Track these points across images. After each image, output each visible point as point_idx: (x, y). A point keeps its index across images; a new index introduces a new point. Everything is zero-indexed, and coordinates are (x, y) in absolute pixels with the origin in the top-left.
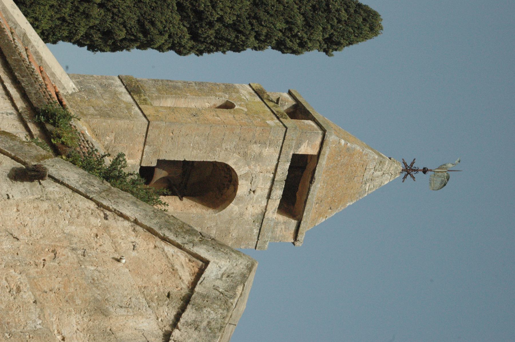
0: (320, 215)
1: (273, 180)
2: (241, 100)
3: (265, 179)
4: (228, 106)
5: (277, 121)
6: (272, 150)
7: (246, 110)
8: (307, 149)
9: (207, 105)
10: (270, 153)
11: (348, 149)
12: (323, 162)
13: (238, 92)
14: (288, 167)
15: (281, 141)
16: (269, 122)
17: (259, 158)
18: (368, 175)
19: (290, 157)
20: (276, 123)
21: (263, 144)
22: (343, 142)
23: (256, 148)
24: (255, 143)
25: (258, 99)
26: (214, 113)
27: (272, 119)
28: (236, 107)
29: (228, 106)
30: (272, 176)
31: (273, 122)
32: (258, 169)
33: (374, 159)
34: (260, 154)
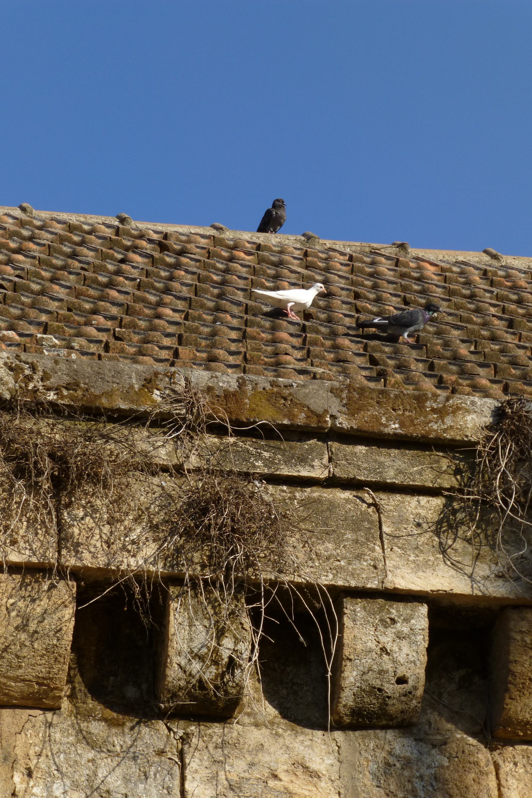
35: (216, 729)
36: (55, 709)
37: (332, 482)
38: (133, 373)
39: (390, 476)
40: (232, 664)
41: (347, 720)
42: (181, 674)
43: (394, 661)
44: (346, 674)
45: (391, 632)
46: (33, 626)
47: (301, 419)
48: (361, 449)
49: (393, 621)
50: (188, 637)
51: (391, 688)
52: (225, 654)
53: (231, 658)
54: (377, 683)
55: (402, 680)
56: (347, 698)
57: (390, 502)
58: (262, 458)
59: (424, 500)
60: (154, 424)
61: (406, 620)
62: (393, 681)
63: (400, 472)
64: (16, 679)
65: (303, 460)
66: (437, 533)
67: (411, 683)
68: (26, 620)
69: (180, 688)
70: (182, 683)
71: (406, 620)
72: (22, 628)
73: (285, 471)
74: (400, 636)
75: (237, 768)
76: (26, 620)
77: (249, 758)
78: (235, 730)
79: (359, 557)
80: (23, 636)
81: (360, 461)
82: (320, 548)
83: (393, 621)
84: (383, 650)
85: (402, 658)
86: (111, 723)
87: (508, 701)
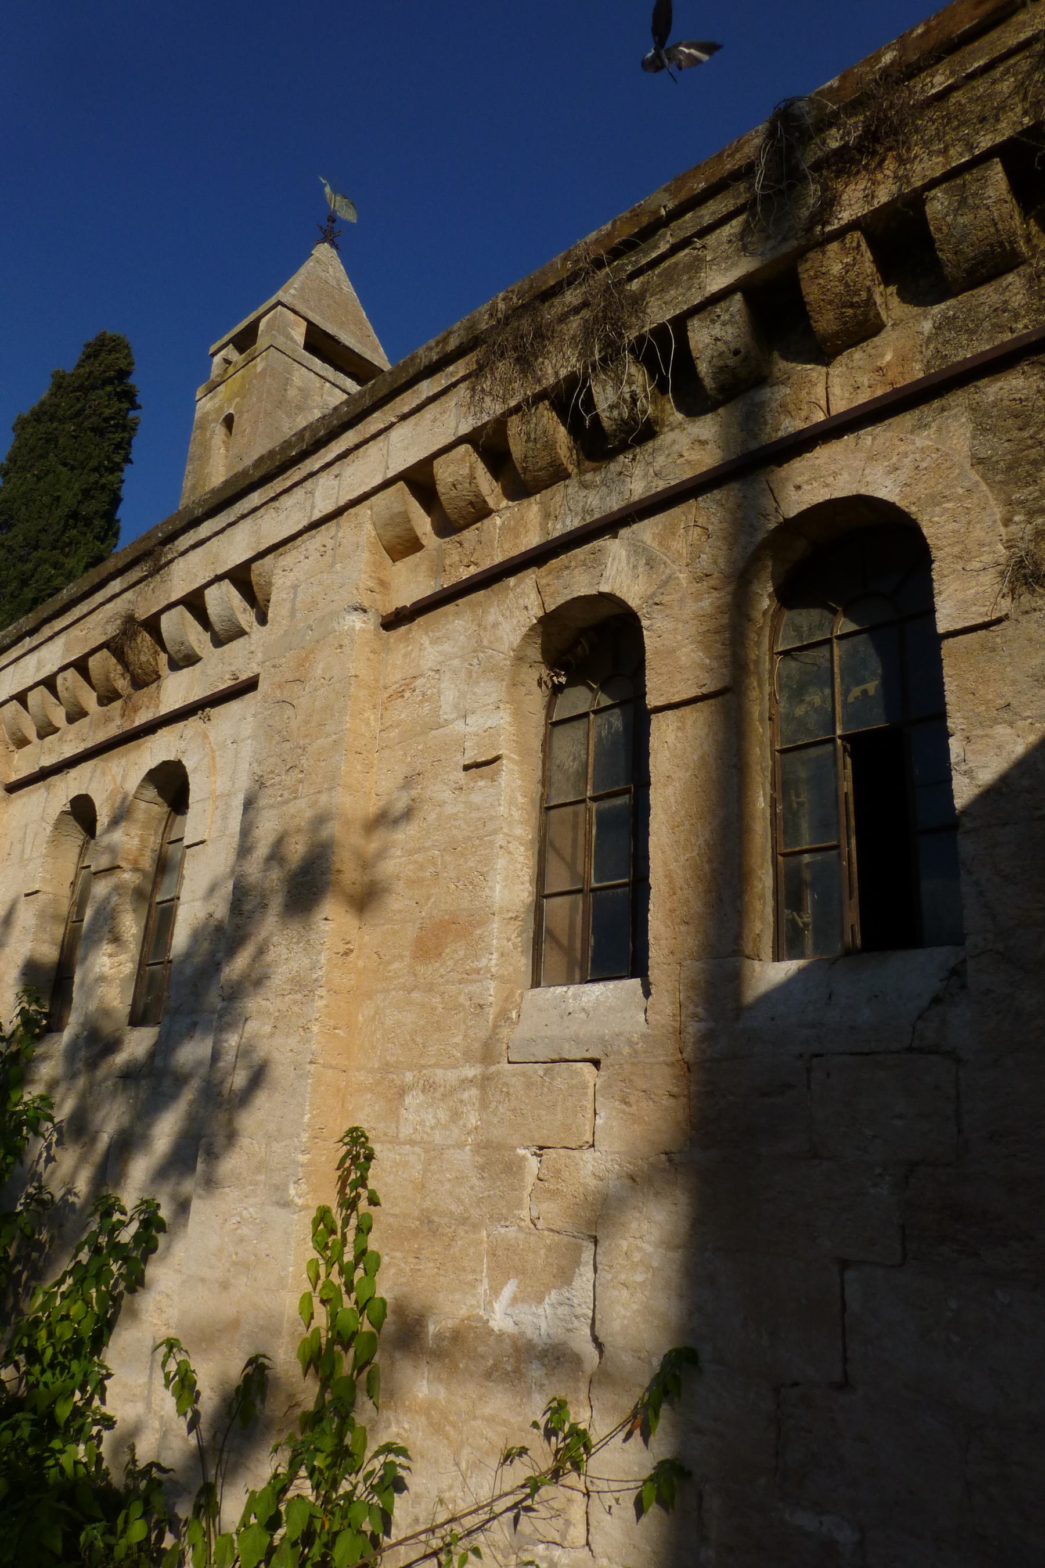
0: (376, 350)
1: (333, 384)
2: (221, 408)
3: (331, 394)
4: (229, 422)
5: (258, 359)
6: (296, 374)
7: (237, 399)
8: (299, 333)
9: (222, 451)
10: (300, 377)
11: (302, 289)
12: (317, 320)
13: (208, 413)
14: (319, 362)
15: (287, 358)
16: (259, 369)
17: (305, 392)
18: (334, 283)
19: (307, 354)
20: (262, 360)
21: (287, 382)
22: (292, 291)
23: (292, 393)
24: (285, 390)
25: (221, 388)
26: (239, 437)
27: (255, 366)
28: (232, 411)
29: (229, 422)
30: (328, 384)
31: (259, 364)
32: (318, 399)
33: (314, 267)
34: (300, 389)
35: (650, 444)
36: (568, 476)
37: (674, 249)
38: (557, 261)
39: (707, 220)
40: (634, 399)
41: (720, 397)
42: (611, 422)
43: (725, 343)
44: (699, 369)
45: (718, 325)
46: (533, 436)
47: (645, 220)
48: (690, 215)
49: (719, 316)
50: (605, 397)
51: (731, 362)
52: (627, 396)
53: (631, 397)
54: (721, 363)
55: (736, 353)
56: (708, 383)
57: (711, 239)
58: (628, 264)
59: (734, 222)
60: (570, 284)
61: (727, 311)
62: (731, 355)
63: (713, 213)
64: (540, 470)
65: (656, 247)
66: (741, 239)
67: (742, 350)
68: (528, 434)
69: (615, 430)
70: (614, 427)
71: (727, 311)
72: (528, 440)
73: (644, 262)
74: (724, 324)
75: (661, 460)
76: (528, 434)
77: (667, 452)
78: (658, 442)
79: (690, 289)
80: (531, 445)
81: (689, 222)
82: (667, 298)
83: (719, 316)
84: (717, 339)
85: (729, 338)
86: (594, 470)
87: (814, 325)
